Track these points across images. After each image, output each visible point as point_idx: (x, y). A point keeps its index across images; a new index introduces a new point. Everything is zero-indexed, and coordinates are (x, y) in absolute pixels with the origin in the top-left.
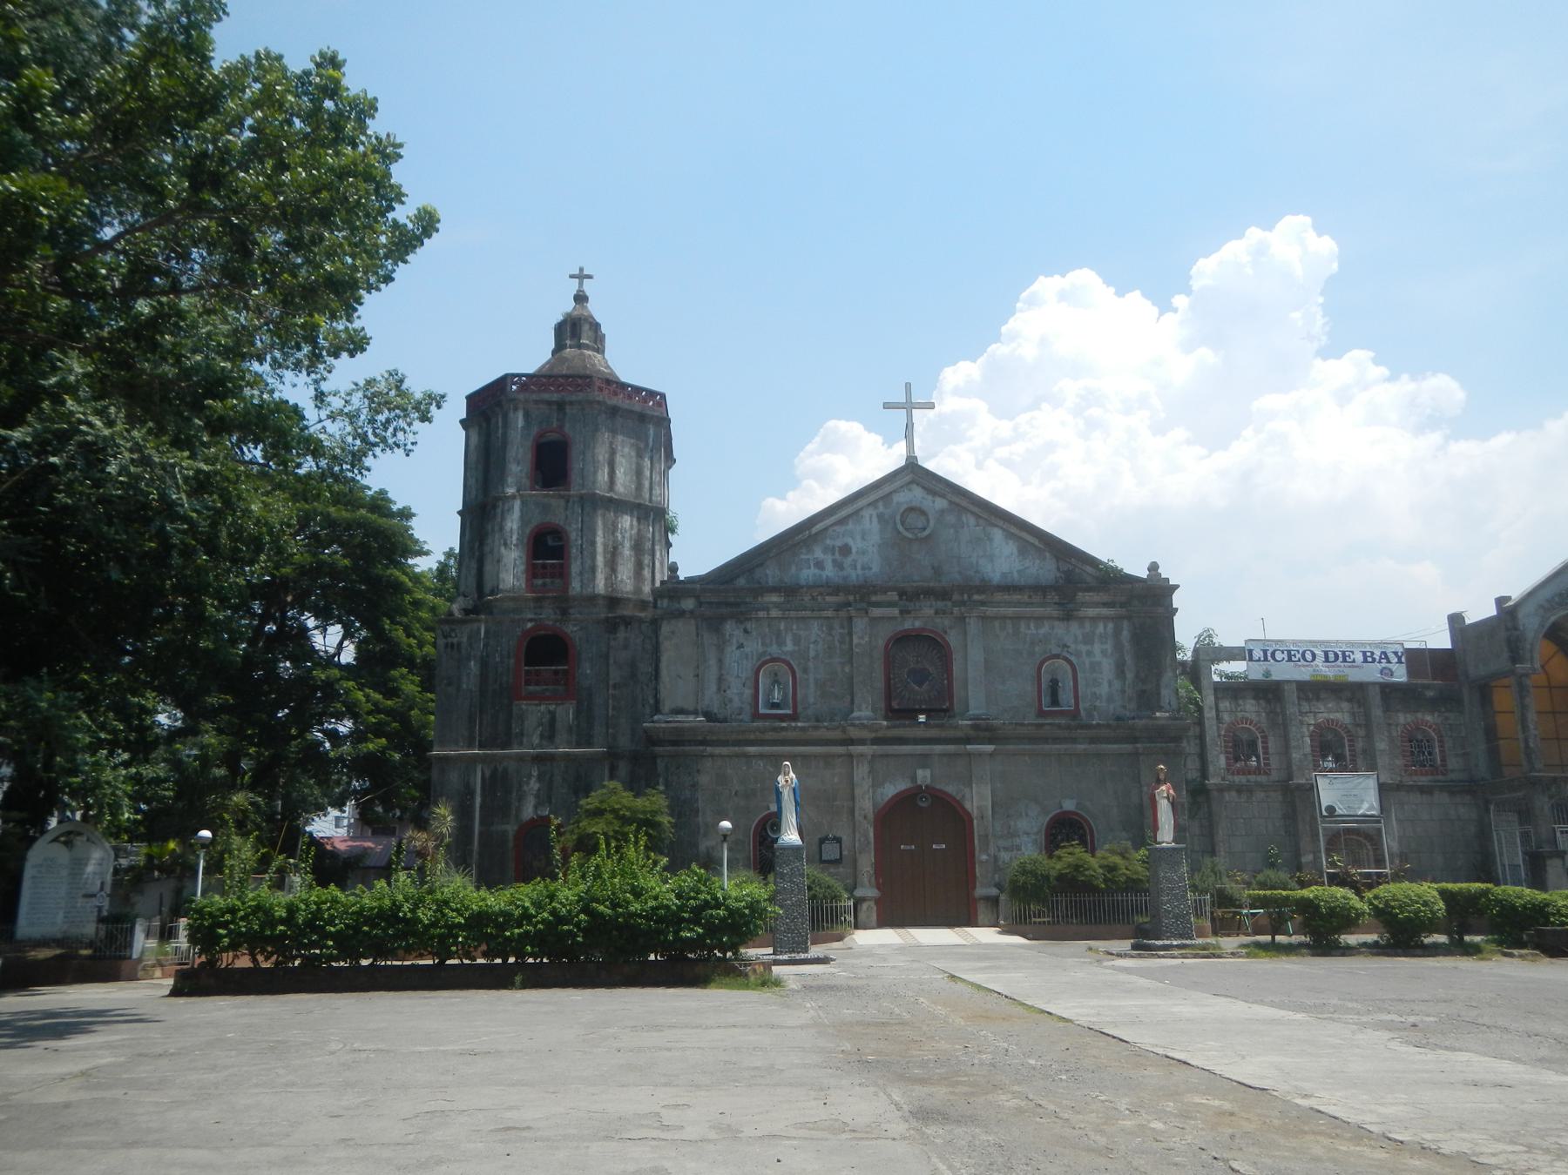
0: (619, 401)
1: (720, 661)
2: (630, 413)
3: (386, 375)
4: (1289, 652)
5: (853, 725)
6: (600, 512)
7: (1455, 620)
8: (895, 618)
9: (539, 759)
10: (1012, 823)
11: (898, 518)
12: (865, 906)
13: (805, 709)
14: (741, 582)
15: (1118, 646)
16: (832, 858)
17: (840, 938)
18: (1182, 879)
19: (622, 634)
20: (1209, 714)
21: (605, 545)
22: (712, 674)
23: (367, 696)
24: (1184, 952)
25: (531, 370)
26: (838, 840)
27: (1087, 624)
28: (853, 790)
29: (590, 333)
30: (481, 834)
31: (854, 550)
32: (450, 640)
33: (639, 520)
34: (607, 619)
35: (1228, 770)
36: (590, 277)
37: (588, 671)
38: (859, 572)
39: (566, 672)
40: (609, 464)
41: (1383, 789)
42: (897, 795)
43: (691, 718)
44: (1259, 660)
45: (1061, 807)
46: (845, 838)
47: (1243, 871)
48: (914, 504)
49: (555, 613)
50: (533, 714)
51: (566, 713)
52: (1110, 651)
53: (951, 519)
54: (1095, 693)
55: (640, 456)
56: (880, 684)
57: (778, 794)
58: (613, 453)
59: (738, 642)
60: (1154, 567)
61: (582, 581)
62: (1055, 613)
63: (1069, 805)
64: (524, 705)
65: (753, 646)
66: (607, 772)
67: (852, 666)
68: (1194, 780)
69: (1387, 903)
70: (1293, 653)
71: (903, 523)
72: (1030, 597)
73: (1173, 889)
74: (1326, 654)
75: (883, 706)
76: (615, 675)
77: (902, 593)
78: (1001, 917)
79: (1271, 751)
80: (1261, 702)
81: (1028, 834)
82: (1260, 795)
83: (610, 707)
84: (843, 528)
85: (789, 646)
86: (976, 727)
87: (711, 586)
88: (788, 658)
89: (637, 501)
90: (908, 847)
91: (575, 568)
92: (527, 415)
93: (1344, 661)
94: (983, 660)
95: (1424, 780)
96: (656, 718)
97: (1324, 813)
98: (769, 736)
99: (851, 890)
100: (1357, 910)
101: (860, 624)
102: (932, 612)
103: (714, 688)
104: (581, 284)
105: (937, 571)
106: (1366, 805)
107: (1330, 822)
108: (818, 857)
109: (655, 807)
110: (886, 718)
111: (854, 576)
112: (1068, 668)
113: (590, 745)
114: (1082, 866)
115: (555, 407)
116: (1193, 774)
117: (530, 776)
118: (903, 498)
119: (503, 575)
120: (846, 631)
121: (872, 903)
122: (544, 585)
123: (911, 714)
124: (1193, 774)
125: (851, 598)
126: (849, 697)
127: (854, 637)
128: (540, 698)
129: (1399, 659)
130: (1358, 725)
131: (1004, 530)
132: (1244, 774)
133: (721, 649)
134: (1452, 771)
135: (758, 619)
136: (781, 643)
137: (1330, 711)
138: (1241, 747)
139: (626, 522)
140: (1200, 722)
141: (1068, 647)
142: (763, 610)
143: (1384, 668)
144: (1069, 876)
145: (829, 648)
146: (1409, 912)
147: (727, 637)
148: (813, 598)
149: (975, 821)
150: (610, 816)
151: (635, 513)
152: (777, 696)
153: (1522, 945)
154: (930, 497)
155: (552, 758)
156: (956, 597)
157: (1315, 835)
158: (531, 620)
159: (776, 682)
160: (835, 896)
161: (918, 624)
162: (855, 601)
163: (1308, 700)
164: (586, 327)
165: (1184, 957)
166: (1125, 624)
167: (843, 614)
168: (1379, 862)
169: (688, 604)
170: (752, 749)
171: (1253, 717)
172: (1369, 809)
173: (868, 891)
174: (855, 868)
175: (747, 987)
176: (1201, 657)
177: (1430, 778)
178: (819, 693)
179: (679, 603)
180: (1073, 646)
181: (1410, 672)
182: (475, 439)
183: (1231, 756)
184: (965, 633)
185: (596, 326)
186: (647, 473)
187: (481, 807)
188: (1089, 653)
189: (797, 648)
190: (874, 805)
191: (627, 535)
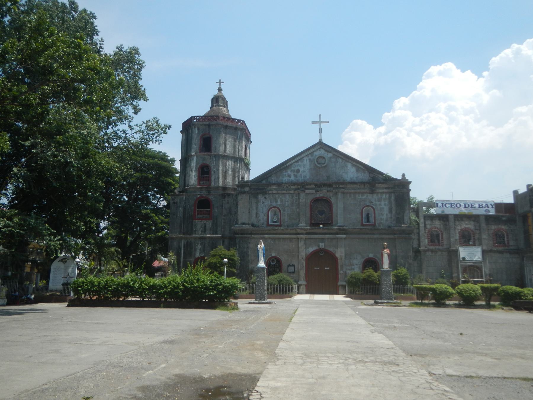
0: (229, 124)
1: (257, 208)
2: (231, 127)
3: (153, 119)
4: (451, 204)
6: (221, 160)
7: (515, 192)
9: (201, 238)
11: (316, 161)
12: (302, 287)
13: (284, 223)
14: (264, 182)
15: (390, 202)
16: (291, 271)
17: (291, 297)
18: (390, 280)
19: (226, 199)
20: (422, 226)
21: (223, 171)
22: (254, 211)
23: (159, 218)
24: (387, 304)
25: (202, 115)
26: (294, 266)
27: (379, 195)
28: (299, 249)
29: (222, 101)
30: (183, 261)
31: (301, 171)
32: (174, 201)
33: (234, 162)
34: (222, 194)
35: (428, 245)
36: (223, 83)
37: (216, 211)
38: (302, 178)
39: (209, 211)
40: (224, 144)
41: (484, 252)
42: (312, 252)
43: (247, 226)
44: (440, 207)
45: (368, 256)
46: (296, 265)
47: (432, 279)
48: (321, 155)
49: (206, 192)
50: (199, 224)
51: (209, 224)
52: (387, 204)
53: (333, 160)
55: (235, 141)
56: (308, 215)
57: (258, 251)
58: (226, 140)
60: (403, 175)
61: (215, 182)
62: (368, 191)
63: (371, 255)
64: (196, 221)
65: (268, 203)
66: (222, 243)
68: (416, 248)
69: (461, 290)
70: (453, 204)
71: (317, 162)
72: (360, 186)
73: (387, 284)
74: (465, 205)
75: (309, 222)
76: (225, 212)
77: (316, 185)
79: (444, 238)
80: (442, 222)
81: (357, 265)
82: (439, 253)
83: (223, 222)
84: (297, 164)
85: (279, 203)
86: (339, 229)
87: (254, 183)
88: (278, 206)
89: (234, 156)
90: (317, 268)
91: (213, 178)
92: (198, 129)
93: (472, 207)
94: (343, 207)
95: (500, 249)
96: (236, 226)
97: (461, 260)
99: (297, 282)
100: (449, 292)
101: (302, 195)
102: (325, 191)
103: (255, 216)
104: (220, 85)
105: (328, 177)
106: (477, 257)
107: (463, 263)
109: (232, 254)
110: (310, 226)
111: (301, 179)
112: (372, 210)
113: (217, 234)
114: (370, 276)
115: (207, 126)
116: (415, 246)
117: (198, 244)
118: (318, 153)
119: (190, 180)
120: (298, 198)
121: (304, 286)
122: (203, 183)
123: (318, 225)
124: (415, 246)
125: (299, 187)
126: (298, 220)
127: (300, 199)
128: (202, 219)
129: (492, 206)
130: (476, 229)
131: (352, 163)
132: (434, 246)
133: (257, 203)
134: (511, 246)
136: (276, 202)
137: (467, 224)
138: (434, 238)
139: (230, 163)
140: (418, 228)
141: (373, 203)
143: (487, 210)
146: (468, 293)
148: (287, 187)
150: (217, 257)
151: (233, 160)
152: (275, 219)
153: (507, 306)
154: (326, 153)
155: (204, 238)
156: (334, 186)
157: (458, 268)
158: (199, 195)
159: (275, 214)
160: (290, 284)
161: (321, 195)
162: (301, 187)
163: (458, 220)
164: (220, 99)
165: (387, 306)
166: (393, 194)
167: (296, 192)
168: (482, 277)
169: (247, 189)
170: (266, 236)
171: (438, 226)
172: (477, 259)
173: (303, 282)
175: (227, 310)
176: (420, 206)
177: (503, 248)
179: (244, 189)
180: (374, 202)
181: (497, 211)
182: (184, 137)
183: (430, 240)
184: (337, 198)
185: (224, 99)
186: (238, 147)
187: (184, 253)
188: (380, 205)
189: (281, 203)
190: (306, 255)
191: (230, 167)
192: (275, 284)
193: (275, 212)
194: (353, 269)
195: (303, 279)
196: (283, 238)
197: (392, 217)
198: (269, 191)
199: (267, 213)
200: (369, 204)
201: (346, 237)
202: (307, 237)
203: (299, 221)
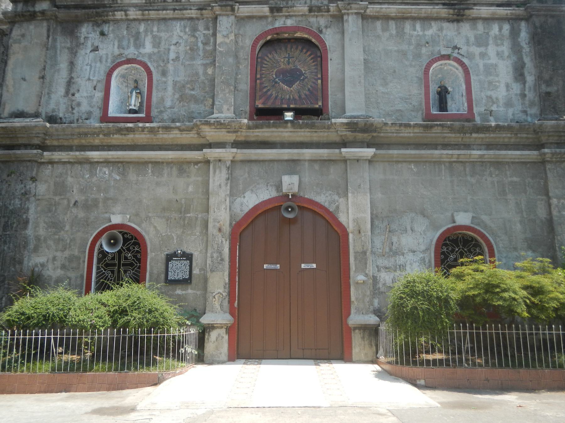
1: (72, 64)
5: (207, 123)
8: (265, 17)
10: (395, 239)
12: (214, 335)
13: (161, 112)
15: (516, 48)
16: (180, 277)
17: (156, 382)
26: (189, 257)
28: (208, 199)
42: (256, 208)
45: (454, 222)
46: (196, 255)
52: (506, 54)
54: (490, 97)
56: (245, 85)
59: (93, 45)
63: (463, 219)
67: (215, 67)
75: (248, 109)
78: (381, 351)
81: (414, 252)
86: (352, 126)
88: (146, 60)
90: (272, 267)
94: (362, 58)
98: (116, 139)
102: (306, 9)
103: (61, 91)
108: (163, 276)
110: (251, 118)
112: (460, 72)
114: (498, 286)
120: (211, 32)
121: (223, 332)
133: (73, 52)
135: (116, 21)
141: (459, 49)
142: (122, 10)
144: (478, 299)
145: (191, 49)
147: (82, 40)
149: (351, 236)
152: (134, 103)
161: (290, 22)
166: (523, 24)
170: (95, 155)
174: (205, 288)
178: (177, 96)
179: (33, 6)
184: (343, 33)
188: (483, 55)
189: (156, 50)
190: (231, 216)
192: (93, 327)
193: (136, 81)
194: (402, 267)
195: (221, 306)
196: (156, 163)
197: (527, 92)
198: (117, 11)
199: (104, 82)
200: (449, 53)
201: (375, 155)
202: (239, 157)
203: (213, 104)
